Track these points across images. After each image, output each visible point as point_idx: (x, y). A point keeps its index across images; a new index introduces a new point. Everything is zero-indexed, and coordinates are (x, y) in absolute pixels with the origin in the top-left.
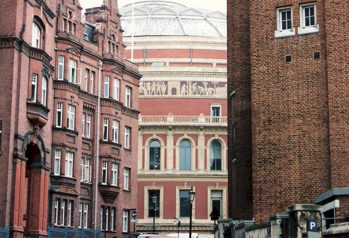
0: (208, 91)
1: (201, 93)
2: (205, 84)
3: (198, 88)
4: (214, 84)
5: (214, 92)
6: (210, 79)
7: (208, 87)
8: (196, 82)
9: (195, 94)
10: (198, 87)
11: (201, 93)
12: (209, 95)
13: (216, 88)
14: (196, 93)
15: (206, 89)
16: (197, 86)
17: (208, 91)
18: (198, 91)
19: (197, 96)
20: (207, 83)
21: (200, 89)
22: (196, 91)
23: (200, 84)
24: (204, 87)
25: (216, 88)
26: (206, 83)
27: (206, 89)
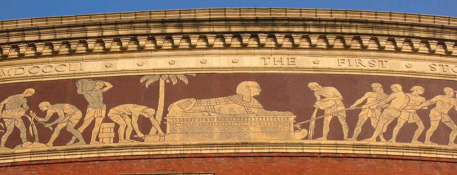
0: (107, 120)
1: (55, 136)
2: (93, 94)
3: (43, 114)
4: (157, 83)
5: (156, 123)
6: (126, 65)
7: (111, 100)
8: (30, 85)
9: (14, 140)
10: (44, 106)
11: (55, 136)
12: (116, 139)
13: (168, 102)
14: (23, 135)
15: (95, 112)
16: (33, 103)
17: (107, 120)
18: (40, 126)
19: (28, 150)
20: (109, 86)
21: (55, 116)
22: (20, 125)
23: (63, 91)
24: (82, 104)
25: (168, 102)
26: (101, 84)
27: (95, 112)
